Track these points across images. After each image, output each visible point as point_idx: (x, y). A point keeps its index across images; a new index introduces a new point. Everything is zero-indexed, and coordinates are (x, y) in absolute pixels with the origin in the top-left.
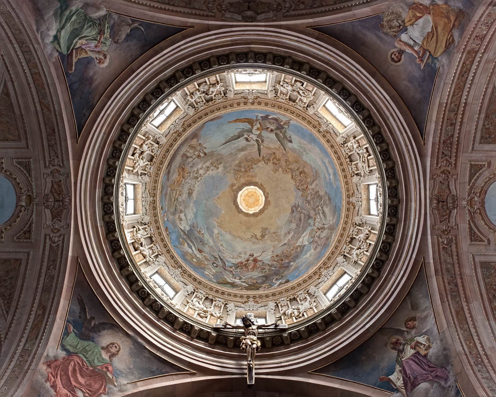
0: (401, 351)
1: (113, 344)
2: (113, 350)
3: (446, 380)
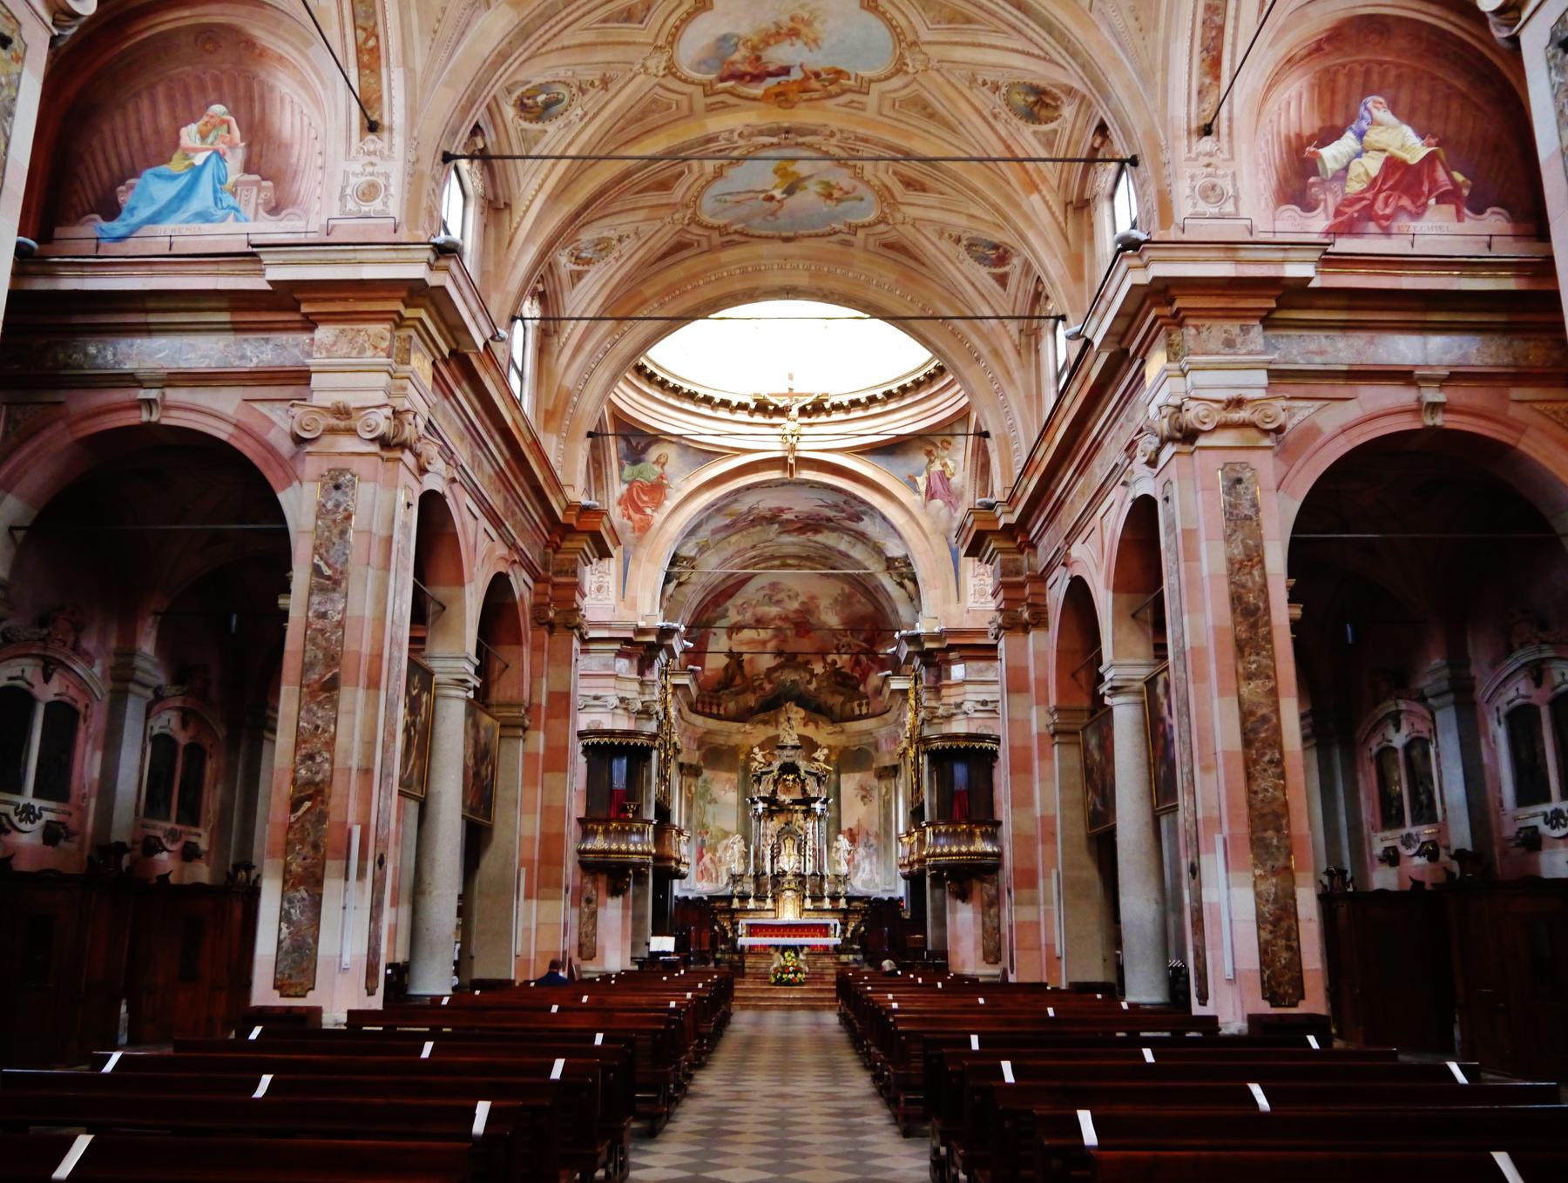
0: (931, 462)
2: (662, 460)
3: (956, 510)
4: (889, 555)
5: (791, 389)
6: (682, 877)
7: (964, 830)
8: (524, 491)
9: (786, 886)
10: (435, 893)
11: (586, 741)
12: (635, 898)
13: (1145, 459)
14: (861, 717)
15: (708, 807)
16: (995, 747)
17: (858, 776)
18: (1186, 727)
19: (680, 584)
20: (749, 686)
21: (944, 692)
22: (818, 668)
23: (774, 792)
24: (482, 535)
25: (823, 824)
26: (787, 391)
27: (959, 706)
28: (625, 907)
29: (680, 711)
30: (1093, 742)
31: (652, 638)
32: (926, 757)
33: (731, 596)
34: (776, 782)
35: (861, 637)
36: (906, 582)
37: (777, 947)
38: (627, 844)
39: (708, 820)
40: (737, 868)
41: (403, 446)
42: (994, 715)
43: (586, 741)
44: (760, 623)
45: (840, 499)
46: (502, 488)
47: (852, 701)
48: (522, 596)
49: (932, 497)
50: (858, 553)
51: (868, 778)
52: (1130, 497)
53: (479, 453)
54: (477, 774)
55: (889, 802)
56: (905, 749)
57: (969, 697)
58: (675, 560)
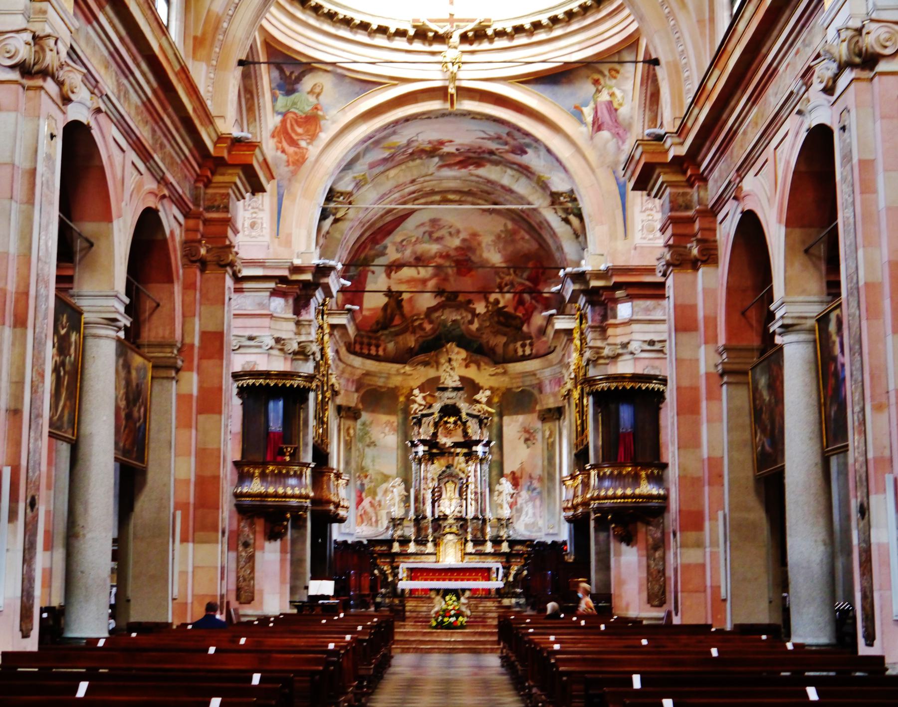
0: (598, 91)
1: (315, 85)
2: (317, 90)
3: (624, 142)
4: (554, 189)
5: (452, 15)
6: (342, 520)
7: (629, 473)
8: (173, 122)
9: (447, 530)
10: (89, 536)
11: (240, 383)
12: (294, 542)
13: (822, 86)
14: (524, 358)
15: (367, 450)
16: (662, 387)
17: (520, 418)
18: (858, 365)
19: (336, 221)
20: (409, 326)
21: (610, 331)
22: (480, 308)
23: (435, 435)
24: (129, 168)
25: (486, 467)
26: (448, 17)
27: (625, 345)
28: (283, 551)
29: (337, 352)
30: (763, 381)
31: (308, 277)
32: (591, 399)
33: (389, 233)
34: (436, 425)
35: (525, 275)
36: (572, 218)
37: (438, 591)
38: (285, 487)
39: (367, 463)
40: (398, 511)
41: (45, 73)
42: (660, 355)
43: (240, 383)
44: (419, 261)
45: (503, 131)
46: (149, 118)
47: (515, 341)
48: (172, 233)
49: (599, 129)
50: (522, 187)
51: (531, 420)
52: (805, 127)
53: (125, 82)
54: (129, 416)
55: (553, 444)
56: (569, 391)
57: (635, 336)
58: (331, 195)
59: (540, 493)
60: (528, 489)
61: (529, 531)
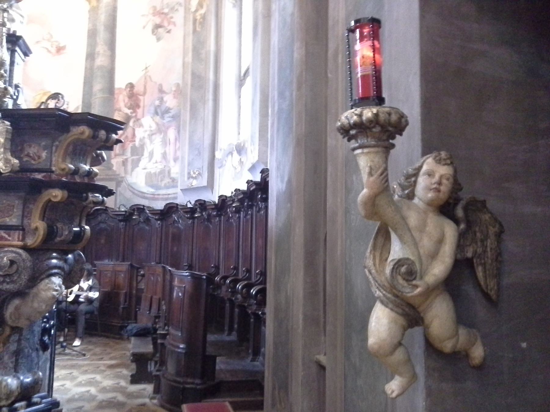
59: (176, 117)
60: (156, 113)
61: (152, 186)
